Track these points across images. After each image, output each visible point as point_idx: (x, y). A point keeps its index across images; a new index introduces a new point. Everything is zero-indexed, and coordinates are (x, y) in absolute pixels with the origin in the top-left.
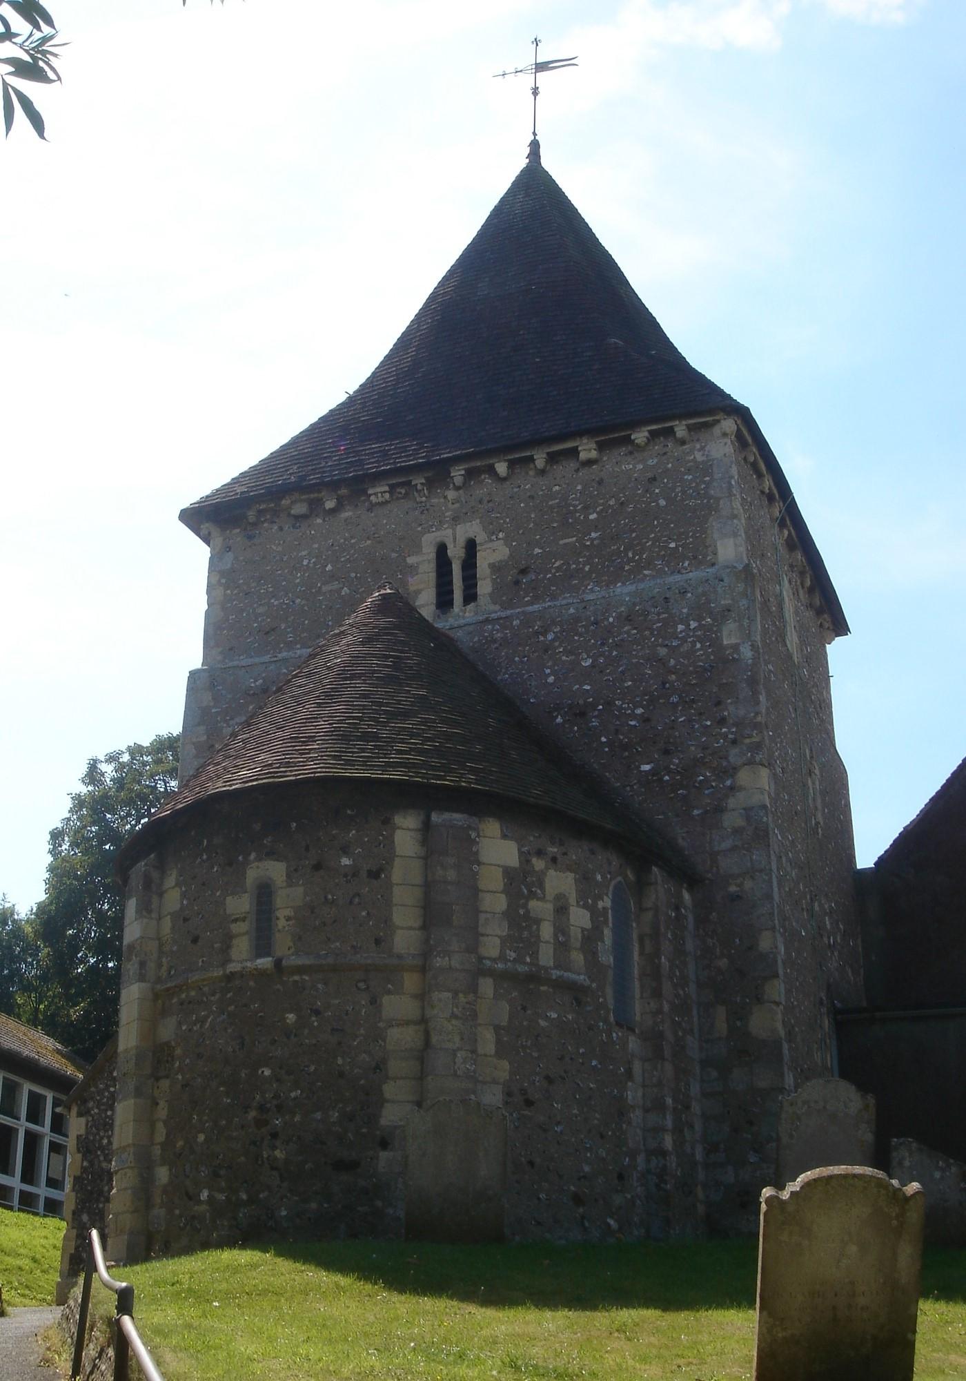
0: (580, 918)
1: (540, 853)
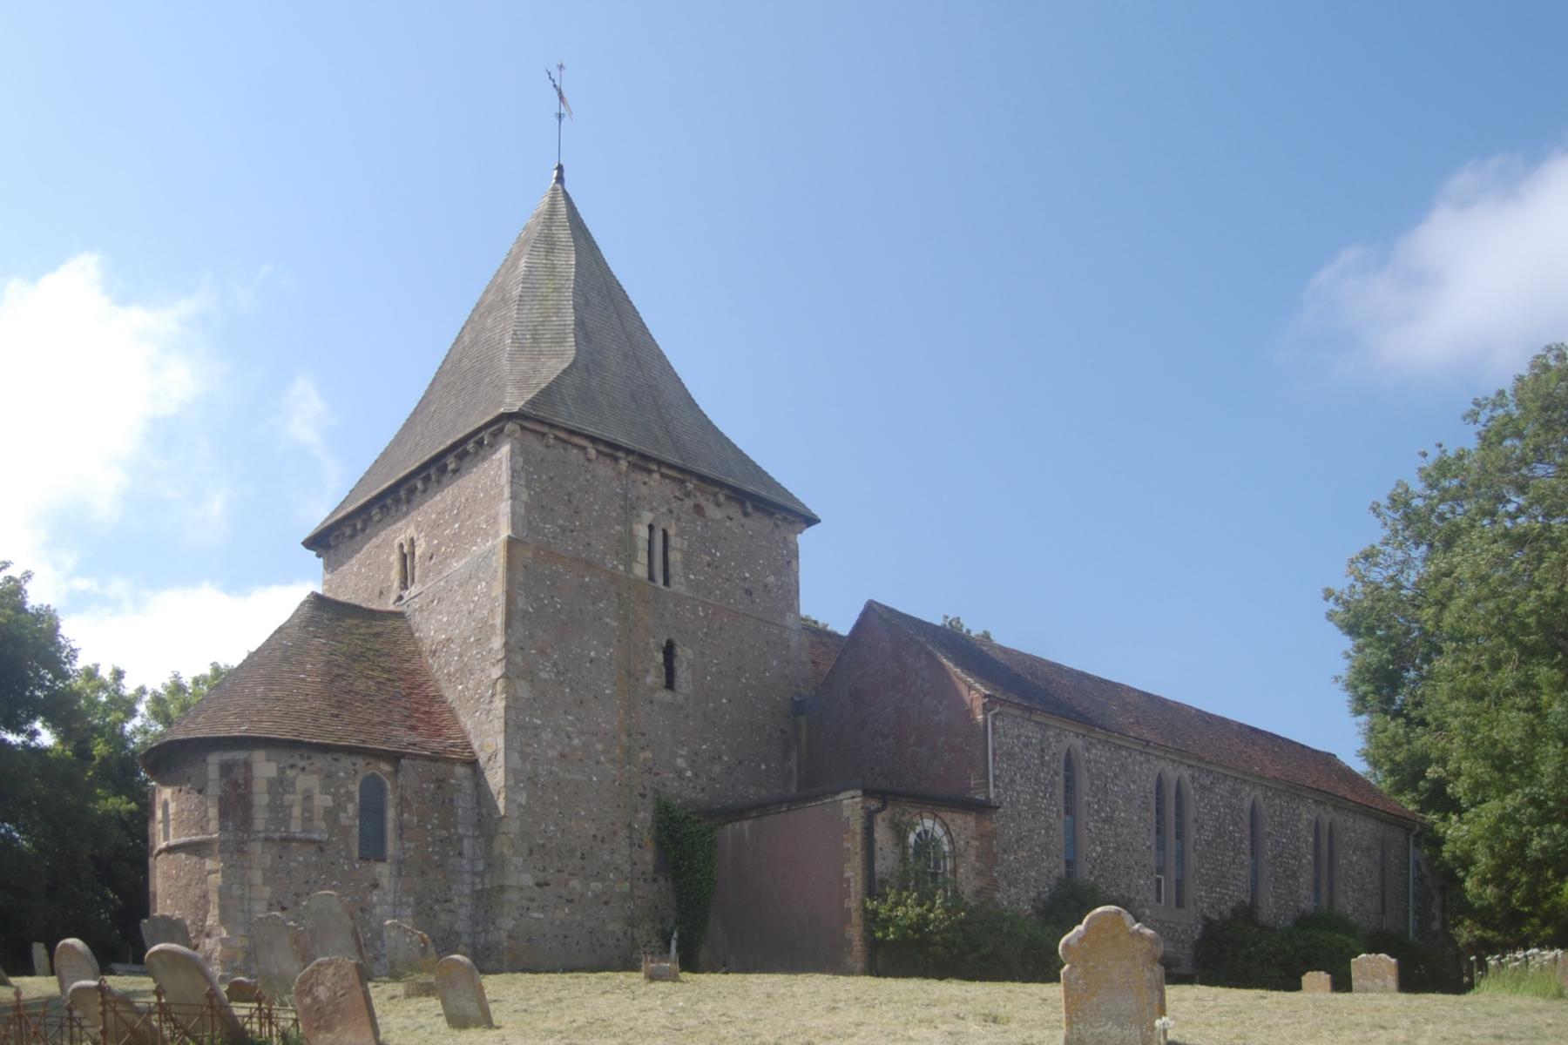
0: (323, 801)
1: (292, 766)
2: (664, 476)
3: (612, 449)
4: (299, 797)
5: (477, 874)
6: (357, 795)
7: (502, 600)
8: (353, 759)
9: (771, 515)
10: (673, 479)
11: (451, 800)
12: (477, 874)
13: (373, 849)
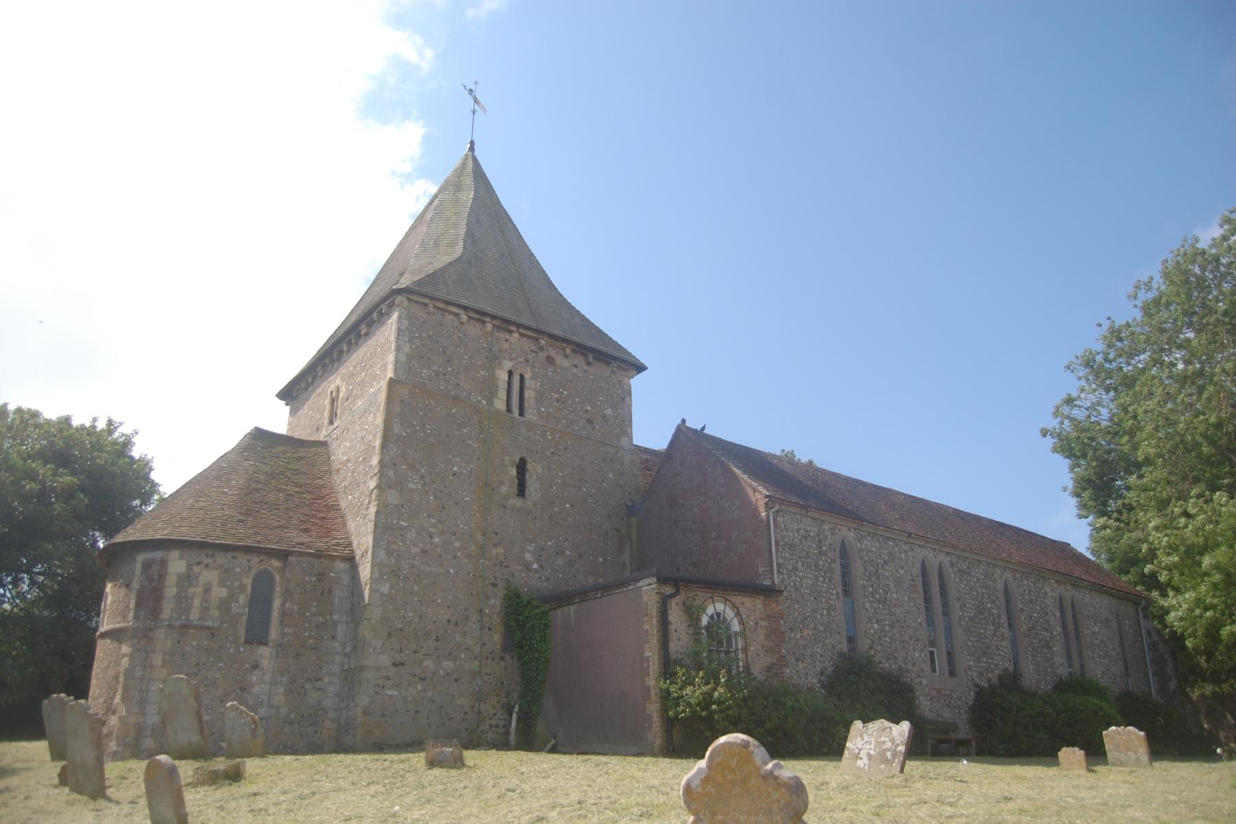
1: (198, 563)
2: (521, 335)
3: (481, 315)
4: (200, 589)
5: (346, 655)
6: (249, 591)
7: (381, 426)
8: (249, 557)
9: (609, 363)
10: (529, 337)
11: (330, 591)
12: (346, 655)
13: (257, 636)
